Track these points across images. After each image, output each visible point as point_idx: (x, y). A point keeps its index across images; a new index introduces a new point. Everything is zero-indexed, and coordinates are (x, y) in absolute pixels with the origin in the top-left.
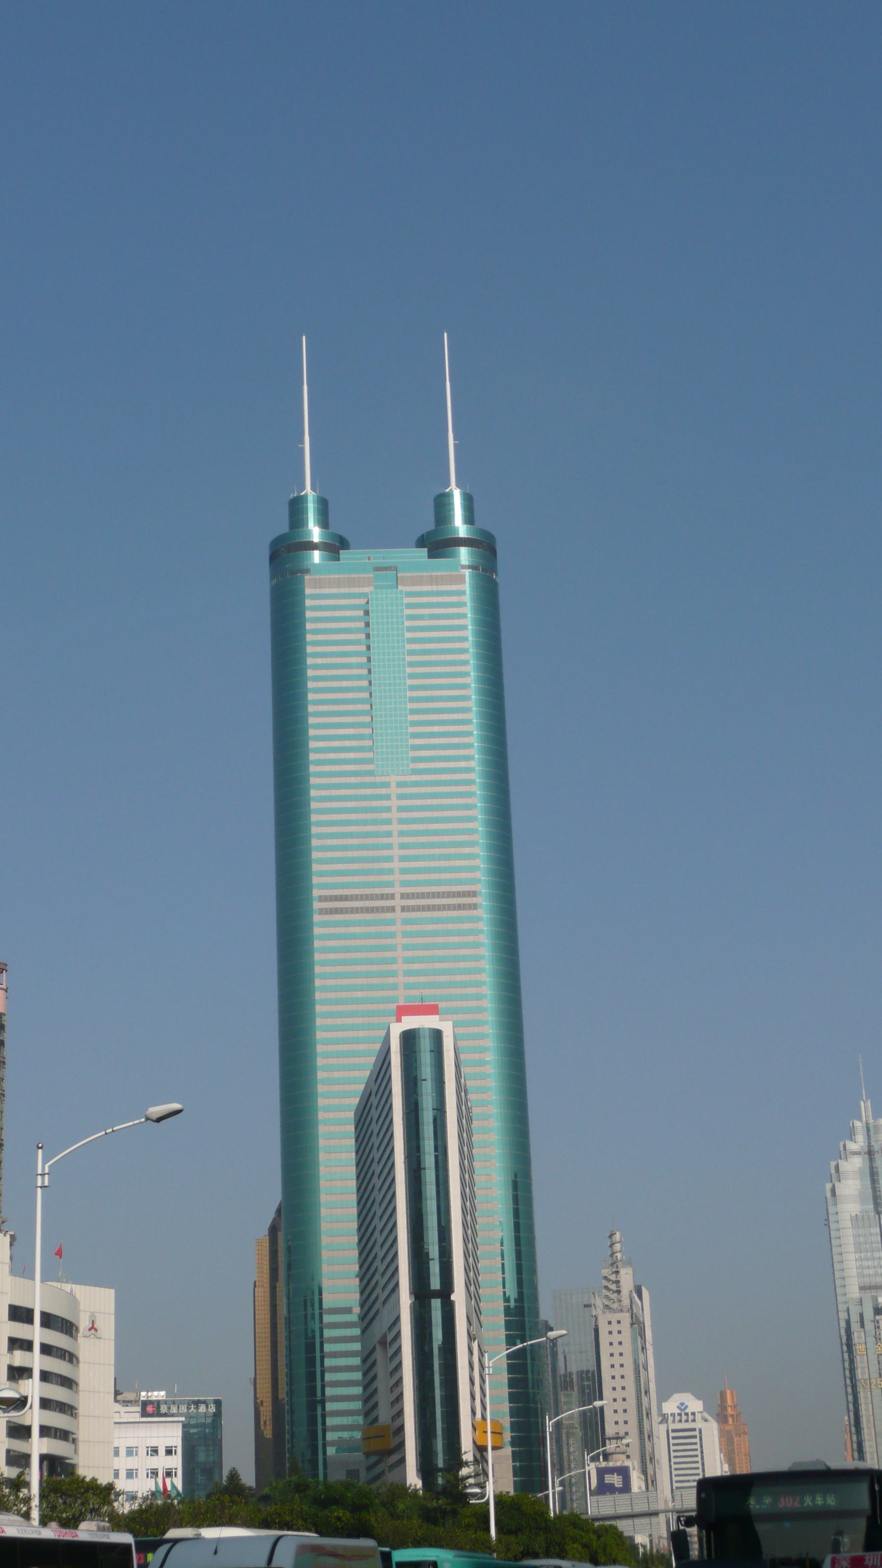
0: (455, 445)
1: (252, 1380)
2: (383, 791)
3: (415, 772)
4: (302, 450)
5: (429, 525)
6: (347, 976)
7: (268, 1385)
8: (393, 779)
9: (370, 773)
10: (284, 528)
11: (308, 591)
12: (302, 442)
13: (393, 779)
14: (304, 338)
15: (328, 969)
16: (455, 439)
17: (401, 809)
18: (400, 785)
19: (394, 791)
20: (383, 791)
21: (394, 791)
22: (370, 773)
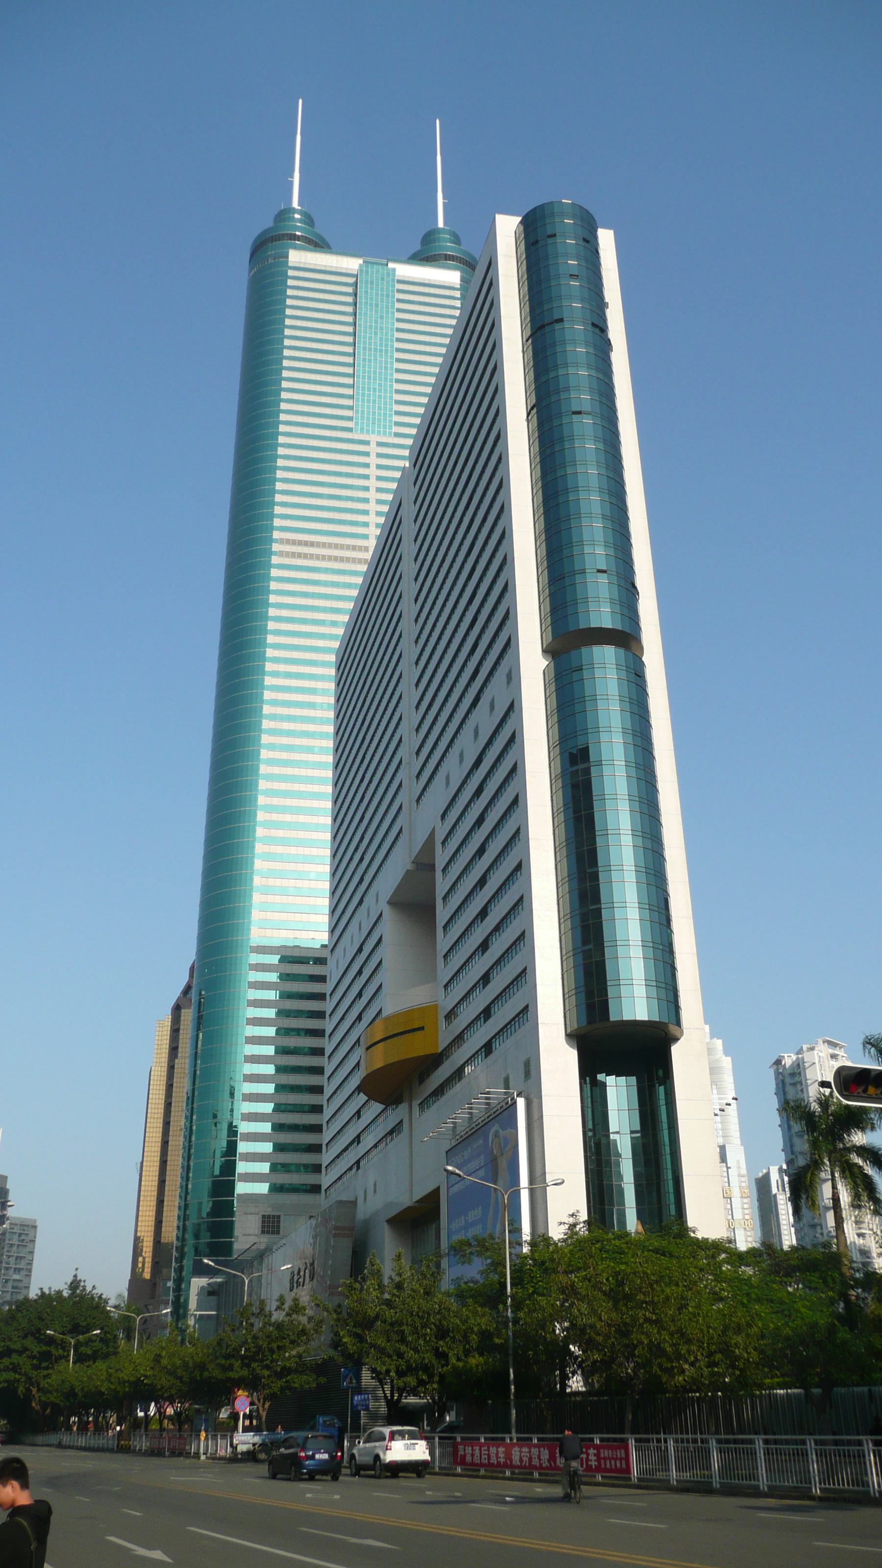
0: (444, 204)
1: (139, 1165)
2: (362, 448)
3: (397, 435)
4: (292, 183)
5: (417, 247)
6: (304, 621)
7: (156, 1148)
8: (374, 438)
9: (350, 430)
10: (270, 223)
11: (290, 264)
12: (292, 177)
13: (374, 438)
14: (300, 101)
15: (285, 613)
16: (444, 198)
17: (379, 467)
18: (380, 444)
19: (373, 449)
20: (362, 448)
21: (373, 449)
22: (350, 430)
